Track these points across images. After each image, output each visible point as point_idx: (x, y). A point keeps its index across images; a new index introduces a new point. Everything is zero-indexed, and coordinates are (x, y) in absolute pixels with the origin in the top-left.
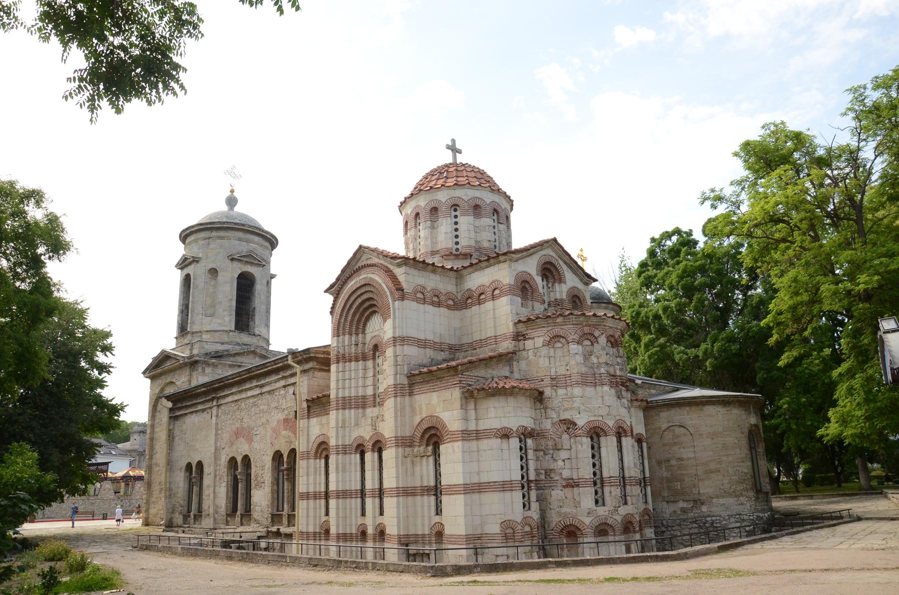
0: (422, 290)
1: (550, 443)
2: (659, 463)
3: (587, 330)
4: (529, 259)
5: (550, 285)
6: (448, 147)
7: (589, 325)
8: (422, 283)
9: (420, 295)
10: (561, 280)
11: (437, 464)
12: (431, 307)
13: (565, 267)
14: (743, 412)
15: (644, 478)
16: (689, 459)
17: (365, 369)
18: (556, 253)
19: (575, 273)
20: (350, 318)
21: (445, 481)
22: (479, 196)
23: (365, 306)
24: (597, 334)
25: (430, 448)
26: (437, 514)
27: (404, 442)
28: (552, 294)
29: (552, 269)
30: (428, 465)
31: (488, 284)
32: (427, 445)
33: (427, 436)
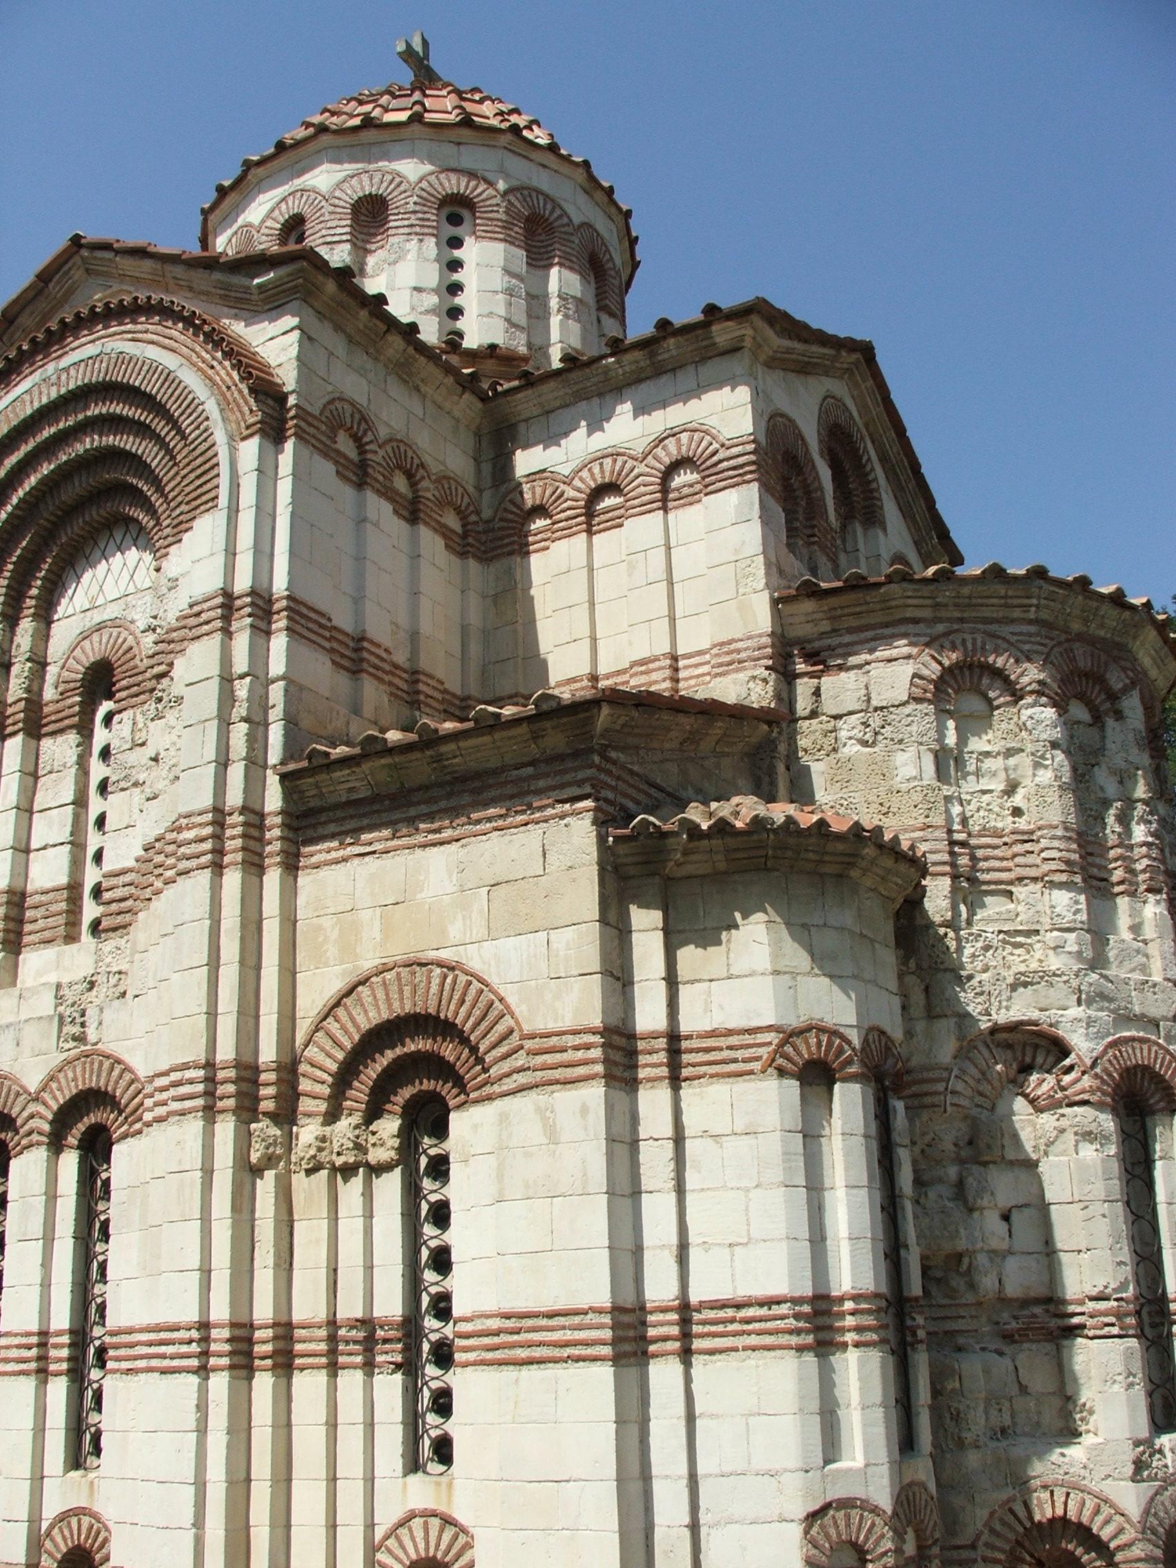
1: (948, 1133)
6: (409, 55)
8: (362, 400)
9: (344, 444)
10: (873, 518)
11: (427, 1215)
12: (386, 508)
13: (879, 472)
17: (32, 774)
19: (906, 512)
21: (471, 1290)
22: (545, 187)
23: (68, 494)
24: (1116, 680)
25: (389, 1126)
26: (413, 1465)
27: (252, 1094)
30: (369, 1215)
31: (639, 447)
32: (373, 1113)
33: (372, 1071)
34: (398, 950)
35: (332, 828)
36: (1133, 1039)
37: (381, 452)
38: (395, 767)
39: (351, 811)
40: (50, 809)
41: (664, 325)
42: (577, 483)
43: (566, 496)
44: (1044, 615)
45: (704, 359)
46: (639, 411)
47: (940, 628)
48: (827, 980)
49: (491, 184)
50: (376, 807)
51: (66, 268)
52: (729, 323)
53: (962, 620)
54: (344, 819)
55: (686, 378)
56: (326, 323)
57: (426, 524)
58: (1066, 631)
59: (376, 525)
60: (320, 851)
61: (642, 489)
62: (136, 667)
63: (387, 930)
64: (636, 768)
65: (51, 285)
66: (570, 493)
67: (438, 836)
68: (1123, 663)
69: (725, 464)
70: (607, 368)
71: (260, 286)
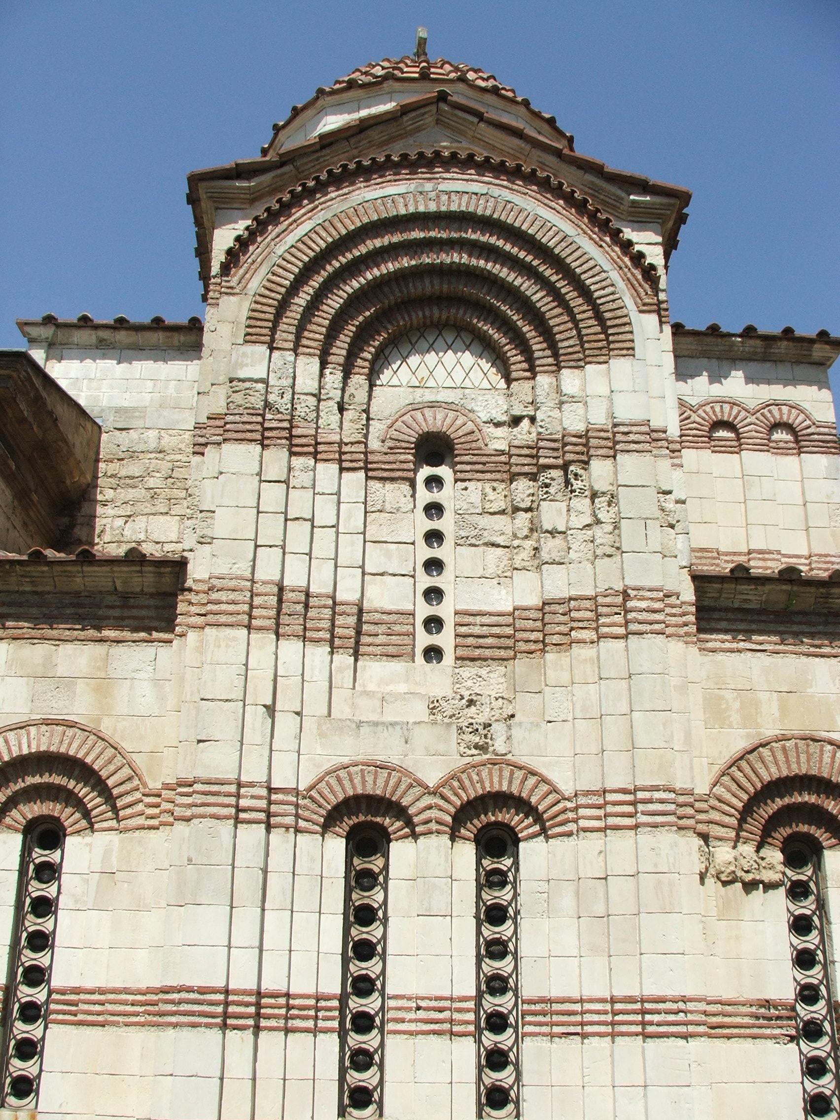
20: (334, 302)
23: (415, 289)
34: (795, 726)
35: (724, 625)
38: (789, 594)
39: (740, 616)
40: (386, 542)
41: (788, 331)
42: (700, 412)
43: (692, 419)
45: (798, 363)
46: (749, 380)
50: (763, 618)
51: (422, 111)
52: (827, 347)
54: (735, 620)
55: (784, 370)
60: (715, 640)
61: (754, 434)
62: (480, 449)
63: (783, 709)
65: (405, 118)
66: (694, 417)
67: (818, 650)
69: (816, 437)
70: (734, 342)
71: (634, 202)
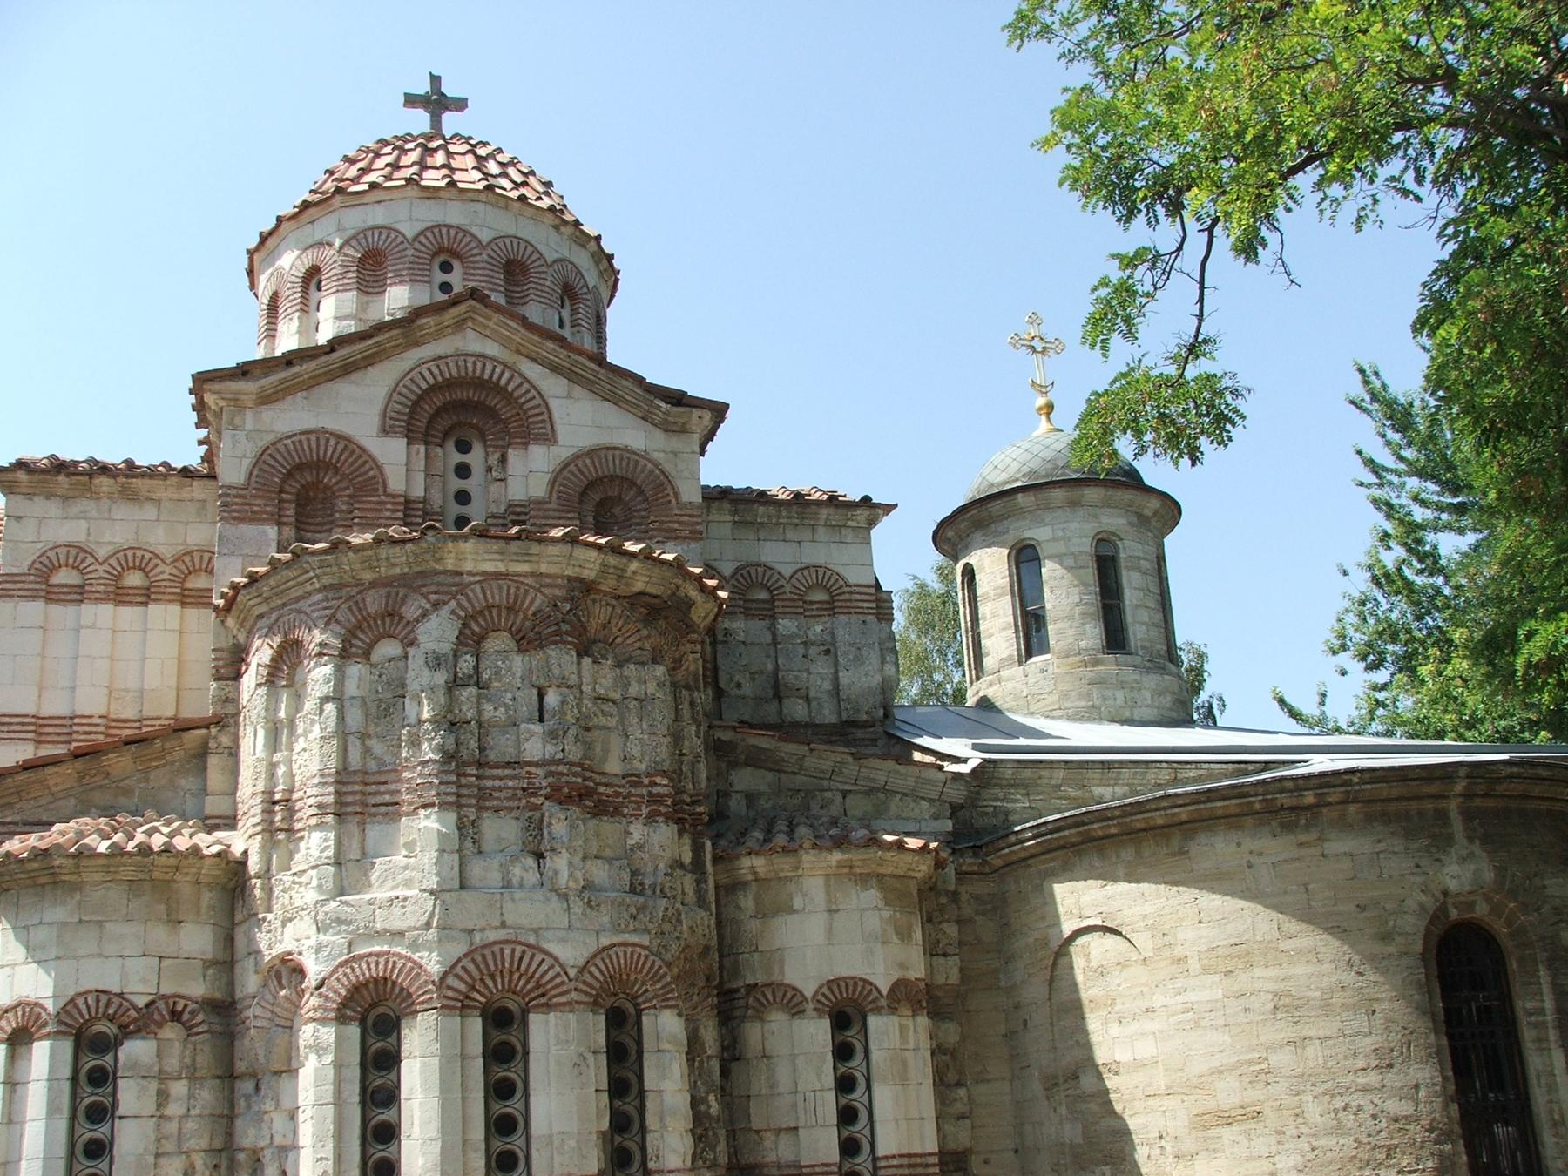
0: (78, 555)
2: (1051, 1084)
3: (374, 602)
4: (344, 388)
5: (494, 459)
6: (411, 101)
7: (388, 582)
9: (64, 577)
14: (1398, 844)
15: (875, 1159)
16: (1138, 1065)
18: (505, 343)
19: (614, 399)
22: (380, 221)
28: (495, 489)
29: (493, 401)
36: (370, 954)
37: (101, 568)
44: (327, 581)
47: (274, 616)
48: (34, 966)
49: (330, 245)
53: (284, 605)
56: (36, 499)
57: (155, 600)
58: (359, 583)
59: (92, 627)
64: (8, 819)
68: (425, 590)
